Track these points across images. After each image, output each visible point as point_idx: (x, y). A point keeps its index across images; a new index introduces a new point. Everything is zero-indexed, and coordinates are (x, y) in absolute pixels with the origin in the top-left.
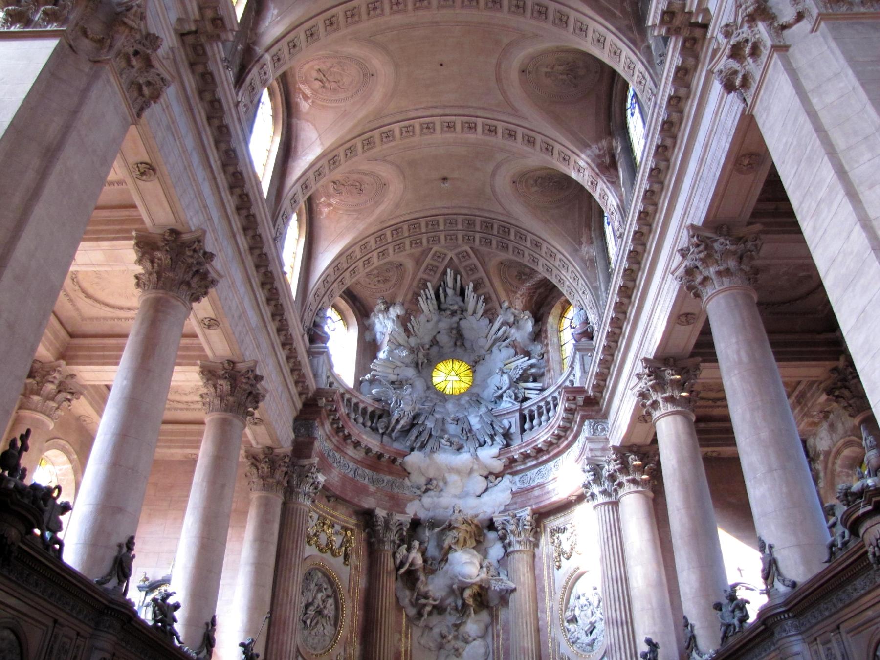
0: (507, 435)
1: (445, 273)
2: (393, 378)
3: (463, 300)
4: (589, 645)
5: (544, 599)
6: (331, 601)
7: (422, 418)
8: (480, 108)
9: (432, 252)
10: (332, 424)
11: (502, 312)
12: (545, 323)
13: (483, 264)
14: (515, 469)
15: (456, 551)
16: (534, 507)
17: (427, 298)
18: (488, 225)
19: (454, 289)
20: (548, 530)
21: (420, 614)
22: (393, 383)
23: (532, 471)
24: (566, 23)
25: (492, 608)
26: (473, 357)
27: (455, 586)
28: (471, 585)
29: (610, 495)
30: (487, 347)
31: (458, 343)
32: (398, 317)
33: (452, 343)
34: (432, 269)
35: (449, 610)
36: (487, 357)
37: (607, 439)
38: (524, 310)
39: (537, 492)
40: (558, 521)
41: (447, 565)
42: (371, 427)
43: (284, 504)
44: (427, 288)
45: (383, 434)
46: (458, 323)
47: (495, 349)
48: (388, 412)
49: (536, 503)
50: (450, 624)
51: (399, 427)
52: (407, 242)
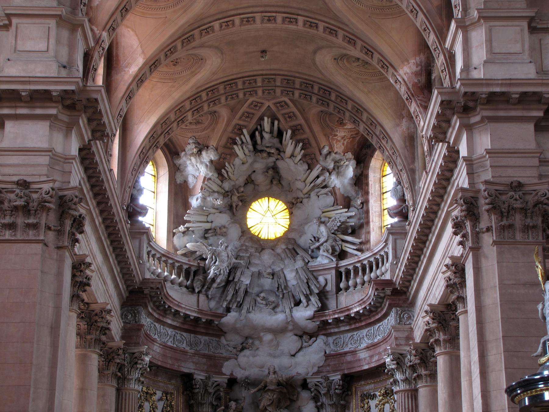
0: (323, 295)
1: (261, 119)
7: (238, 274)
8: (301, 9)
9: (249, 102)
11: (321, 158)
12: (367, 167)
14: (329, 331)
18: (307, 86)
22: (207, 231)
26: (290, 198)
30: (305, 191)
31: (275, 182)
32: (211, 161)
33: (268, 181)
34: (248, 115)
36: (305, 201)
39: (349, 358)
43: (118, 390)
44: (242, 133)
45: (199, 292)
46: (275, 162)
47: (313, 194)
49: (348, 369)
51: (215, 285)
52: (223, 99)
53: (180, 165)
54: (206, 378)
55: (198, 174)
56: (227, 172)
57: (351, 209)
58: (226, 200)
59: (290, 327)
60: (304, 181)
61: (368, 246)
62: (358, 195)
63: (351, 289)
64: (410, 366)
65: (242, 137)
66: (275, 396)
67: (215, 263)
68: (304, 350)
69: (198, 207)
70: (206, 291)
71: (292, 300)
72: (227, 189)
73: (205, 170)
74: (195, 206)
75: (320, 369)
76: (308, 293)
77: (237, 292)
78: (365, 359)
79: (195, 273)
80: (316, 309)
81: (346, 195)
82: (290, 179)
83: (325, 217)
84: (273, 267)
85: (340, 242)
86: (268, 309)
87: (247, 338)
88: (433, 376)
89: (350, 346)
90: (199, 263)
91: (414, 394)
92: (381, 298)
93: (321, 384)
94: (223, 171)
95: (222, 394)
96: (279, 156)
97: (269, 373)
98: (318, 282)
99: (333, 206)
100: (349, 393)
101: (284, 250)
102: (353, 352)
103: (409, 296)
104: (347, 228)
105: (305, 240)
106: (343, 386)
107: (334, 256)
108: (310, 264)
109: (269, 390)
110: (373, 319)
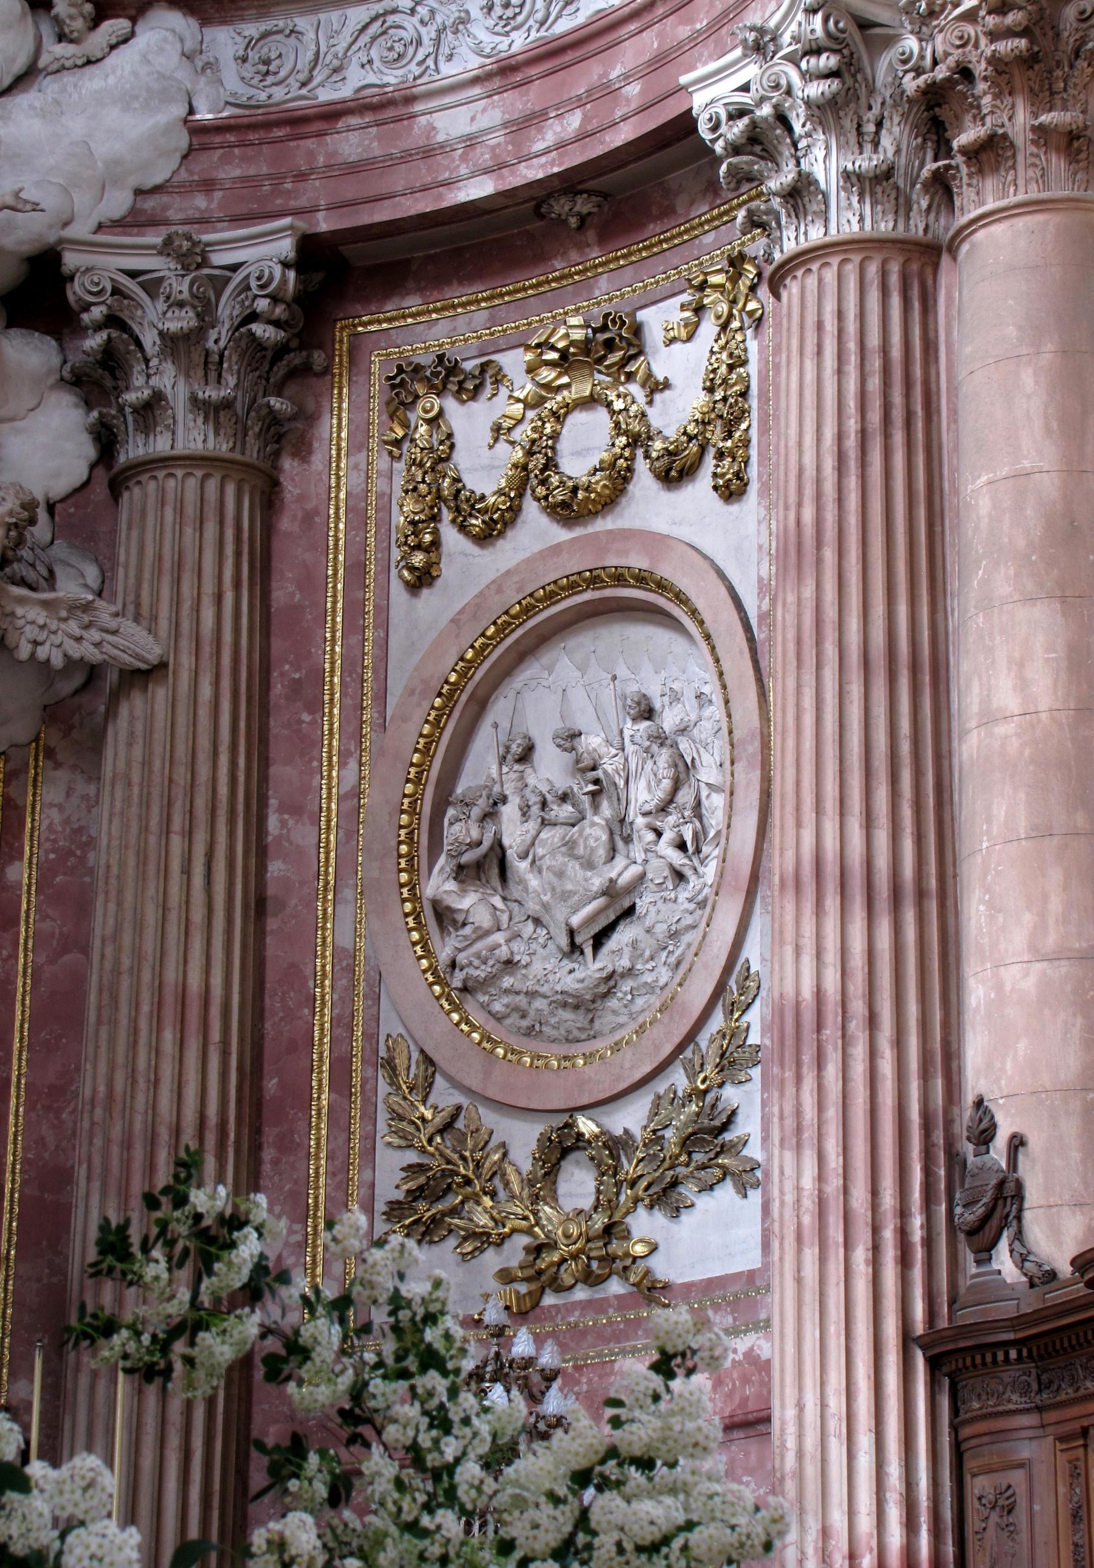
4: (576, 1003)
5: (307, 745)
16: (324, 224)
20: (378, 367)
29: (903, 207)
39: (351, 142)
68: (49, 88)
75: (149, 204)
78: (471, 142)
91: (920, 264)
100: (318, 358)
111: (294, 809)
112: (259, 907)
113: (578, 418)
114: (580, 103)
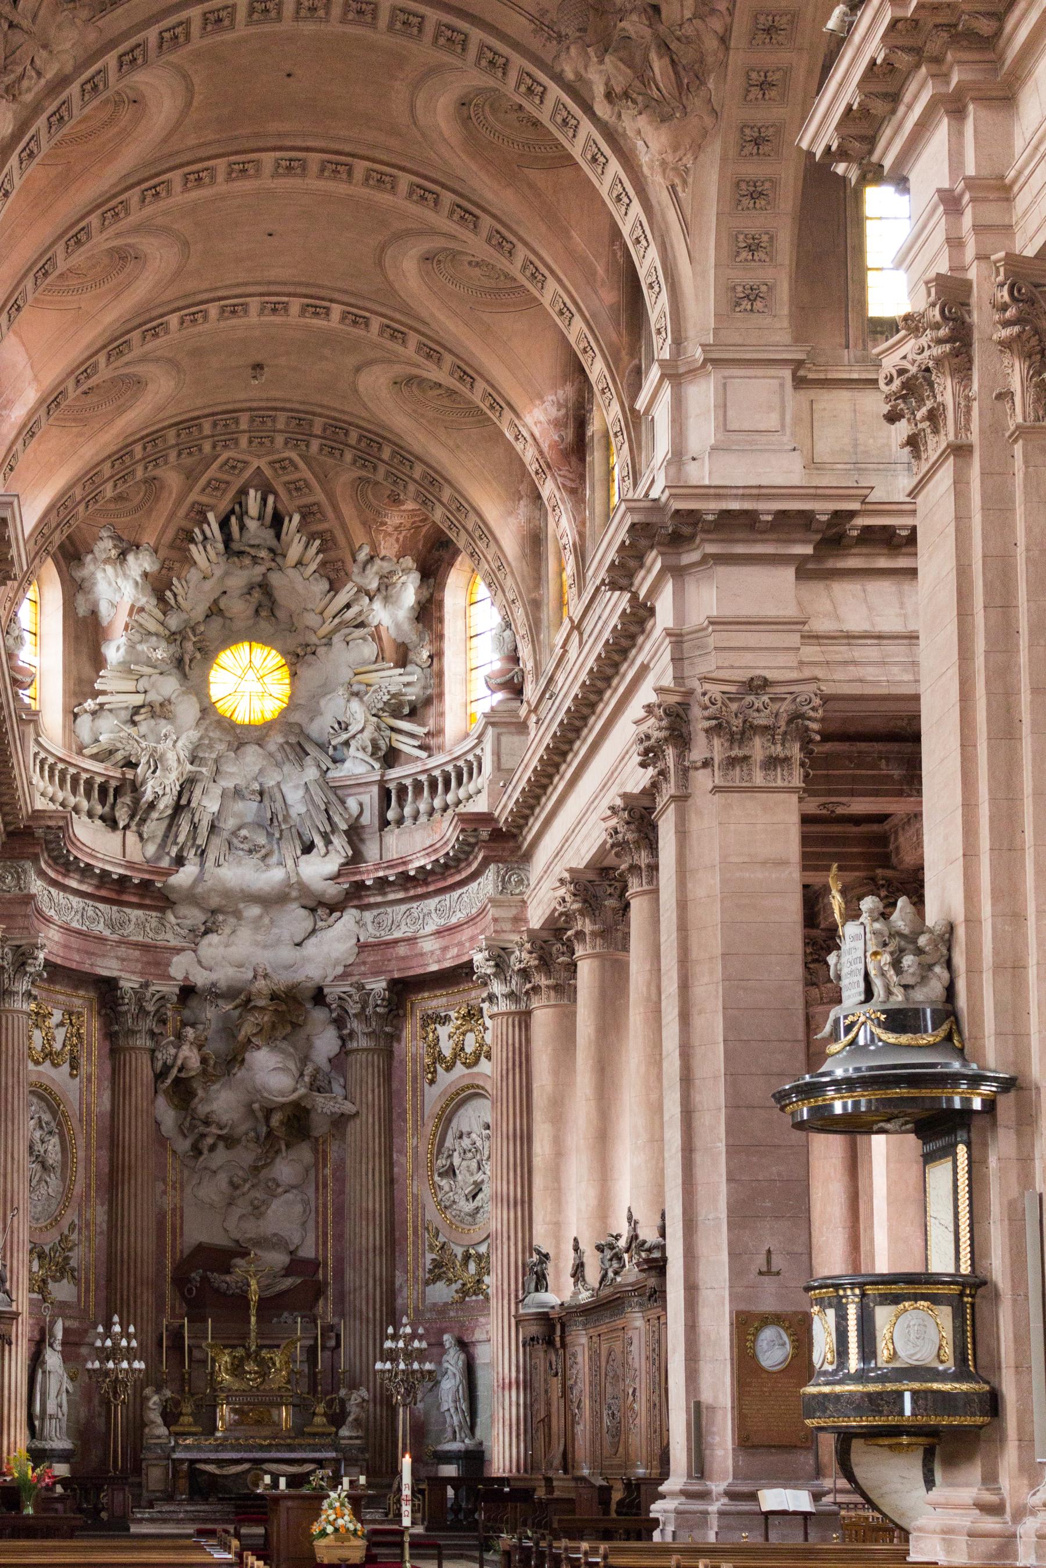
0: (354, 834)
2: (138, 700)
3: (278, 536)
5: (404, 1132)
6: (55, 1140)
10: (50, 851)
13: (324, 479)
14: (366, 901)
15: (259, 1048)
16: (396, 975)
17: (205, 538)
19: (261, 517)
21: (197, 1150)
22: (137, 710)
23: (396, 908)
24: (510, 252)
25: (317, 1139)
26: (292, 643)
27: (256, 1106)
28: (282, 1106)
31: (263, 614)
32: (145, 575)
33: (250, 611)
35: (244, 1143)
36: (321, 651)
37: (524, 902)
38: (400, 555)
39: (402, 950)
40: (434, 1002)
41: (243, 1070)
42: (102, 818)
47: (337, 639)
48: (133, 782)
50: (245, 1166)
53: (83, 580)
54: (141, 987)
55: (118, 599)
56: (175, 595)
57: (410, 668)
58: (173, 648)
59: (294, 894)
60: (321, 613)
61: (440, 740)
62: (422, 639)
63: (408, 822)
64: (519, 970)
65: (205, 526)
66: (266, 1019)
67: (154, 772)
69: (120, 663)
70: (139, 825)
71: (298, 842)
72: (173, 629)
73: (134, 591)
74: (114, 662)
76: (329, 829)
77: (195, 828)
78: (432, 952)
79: (117, 790)
80: (343, 860)
81: (399, 641)
82: (293, 607)
83: (360, 683)
84: (261, 780)
85: (388, 732)
86: (255, 860)
87: (213, 912)
88: (566, 990)
89: (404, 928)
90: (123, 774)
92: (469, 844)
93: (350, 996)
94: (168, 593)
95: (169, 1013)
96: (273, 564)
97: (255, 977)
98: (346, 809)
99: (376, 662)
100: (401, 1012)
101: (282, 745)
102: (411, 940)
103: (522, 843)
104: (401, 705)
105: (321, 727)
106: (390, 1001)
107: (377, 760)
108: (330, 774)
109: (255, 1007)
110: (450, 881)
111: (400, 1152)
112: (391, 1181)
113: (469, 1034)
114: (457, 945)
